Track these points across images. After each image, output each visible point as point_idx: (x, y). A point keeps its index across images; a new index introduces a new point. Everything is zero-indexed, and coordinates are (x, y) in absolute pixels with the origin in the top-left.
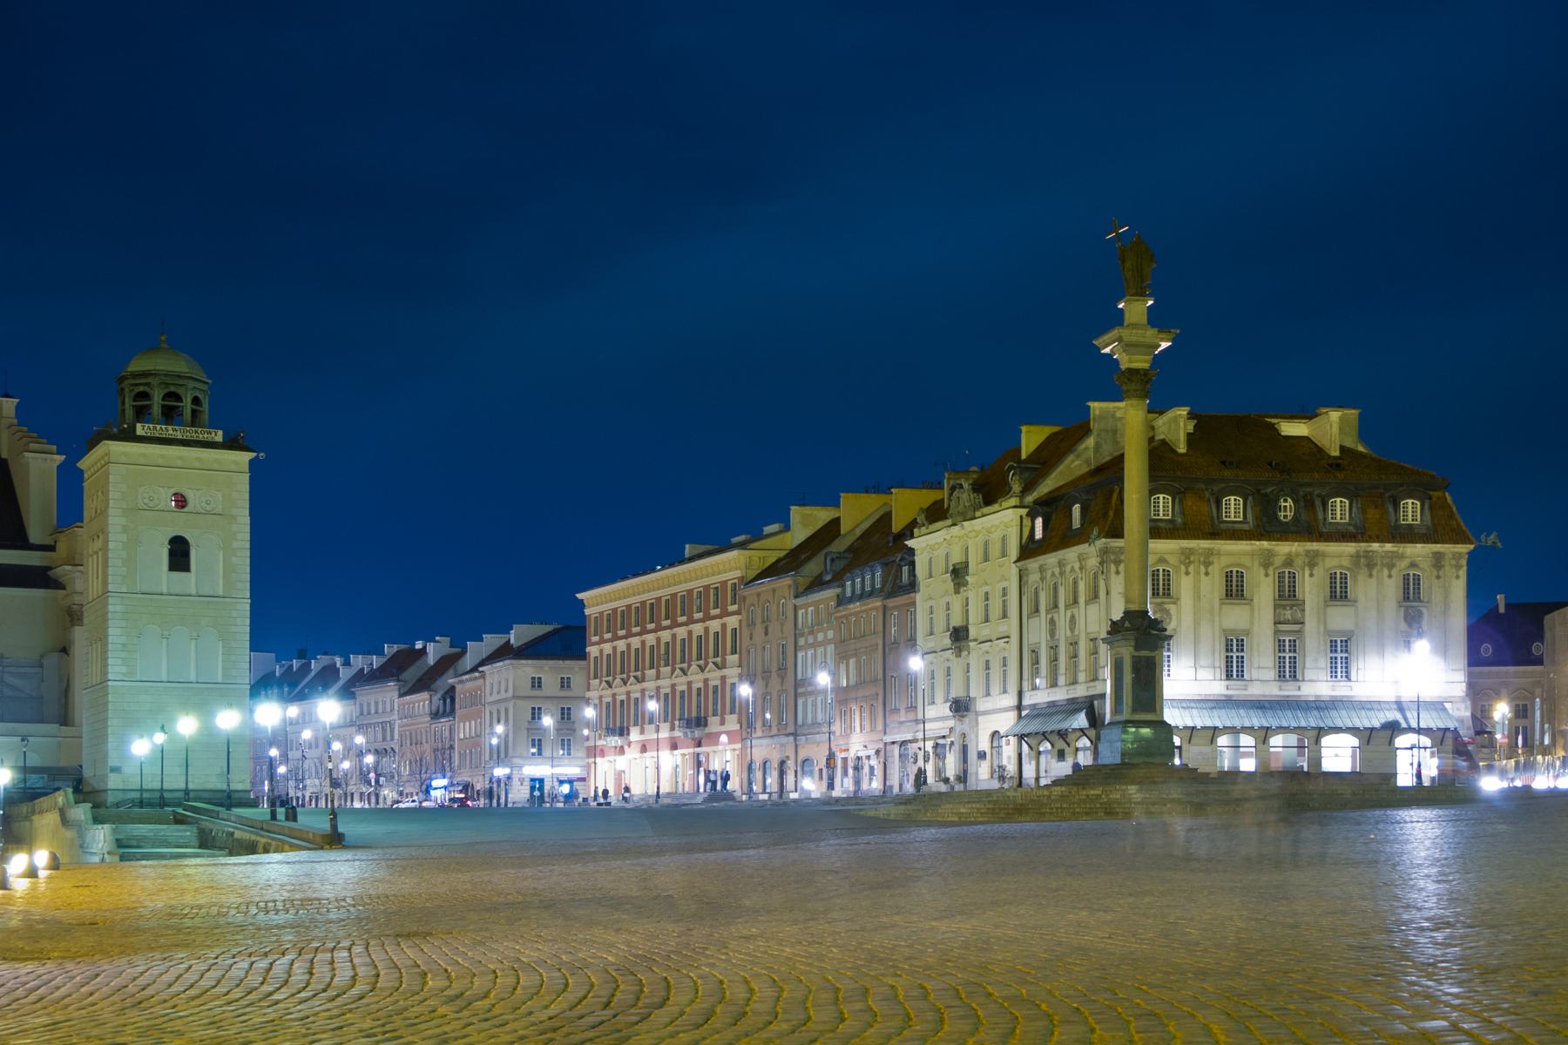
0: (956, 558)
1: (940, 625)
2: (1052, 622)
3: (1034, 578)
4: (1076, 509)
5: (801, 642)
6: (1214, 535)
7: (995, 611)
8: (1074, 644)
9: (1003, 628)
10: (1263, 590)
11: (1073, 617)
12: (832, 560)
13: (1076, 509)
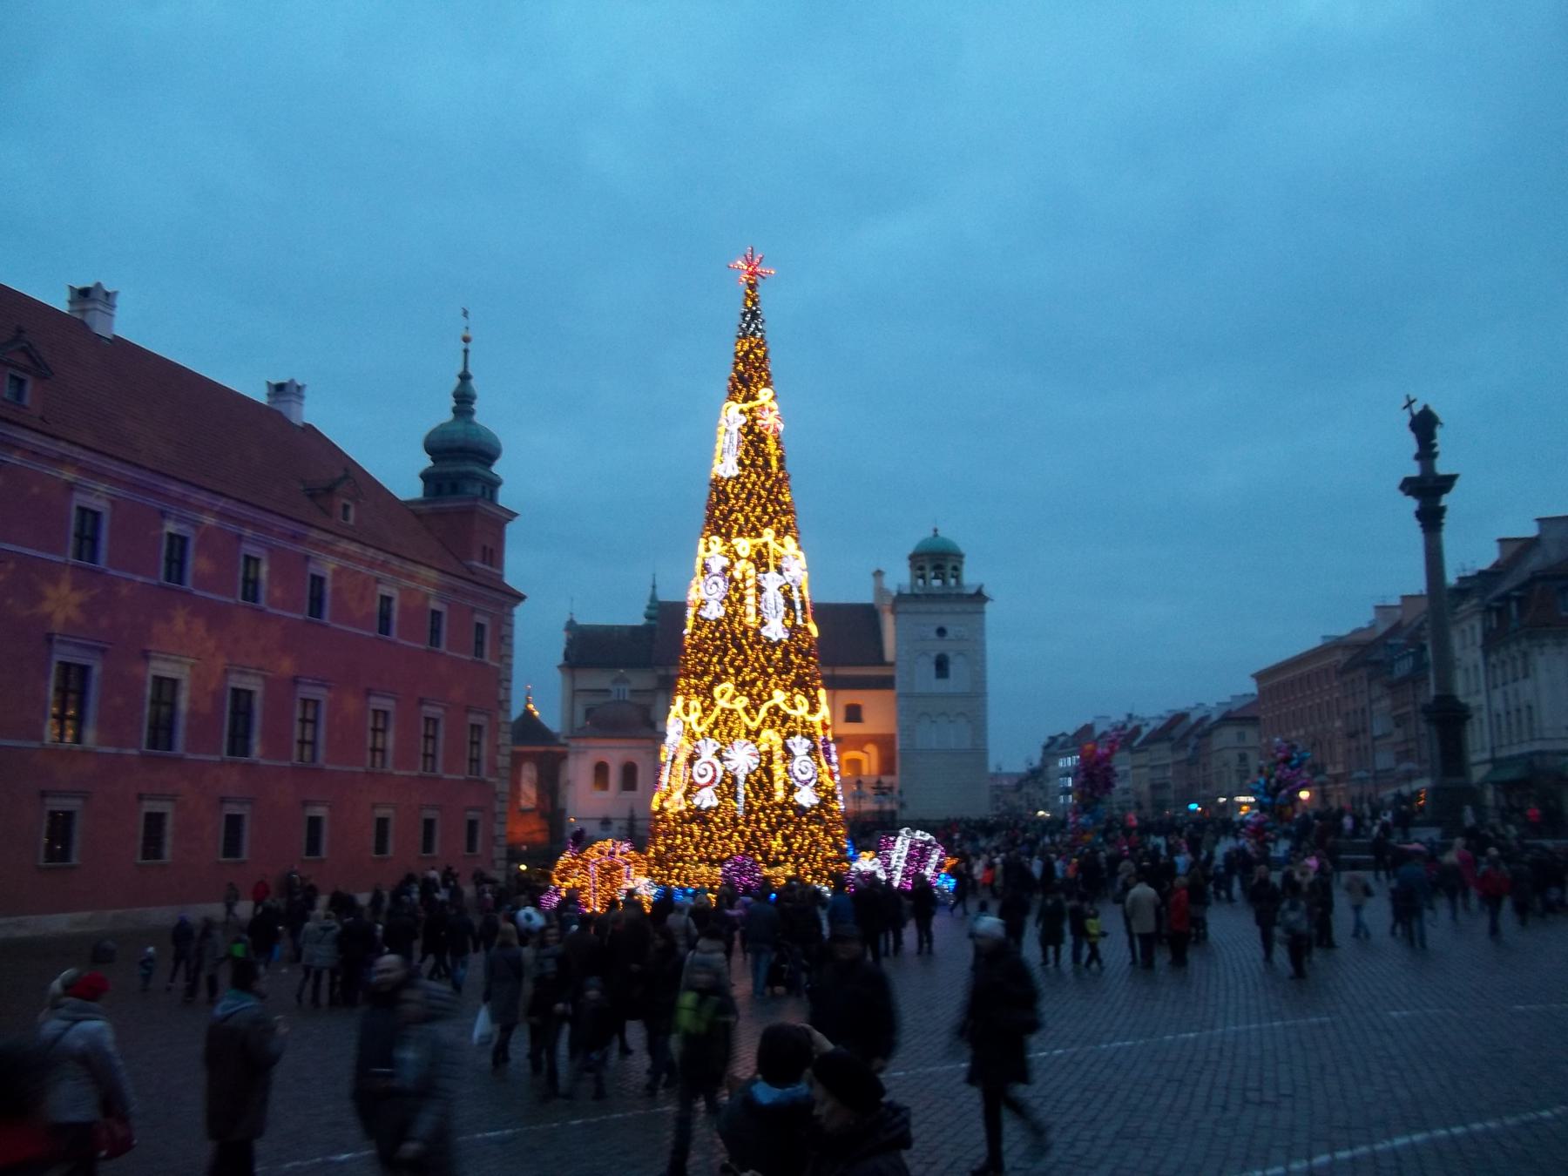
2: (1505, 693)
3: (1493, 659)
8: (1518, 710)
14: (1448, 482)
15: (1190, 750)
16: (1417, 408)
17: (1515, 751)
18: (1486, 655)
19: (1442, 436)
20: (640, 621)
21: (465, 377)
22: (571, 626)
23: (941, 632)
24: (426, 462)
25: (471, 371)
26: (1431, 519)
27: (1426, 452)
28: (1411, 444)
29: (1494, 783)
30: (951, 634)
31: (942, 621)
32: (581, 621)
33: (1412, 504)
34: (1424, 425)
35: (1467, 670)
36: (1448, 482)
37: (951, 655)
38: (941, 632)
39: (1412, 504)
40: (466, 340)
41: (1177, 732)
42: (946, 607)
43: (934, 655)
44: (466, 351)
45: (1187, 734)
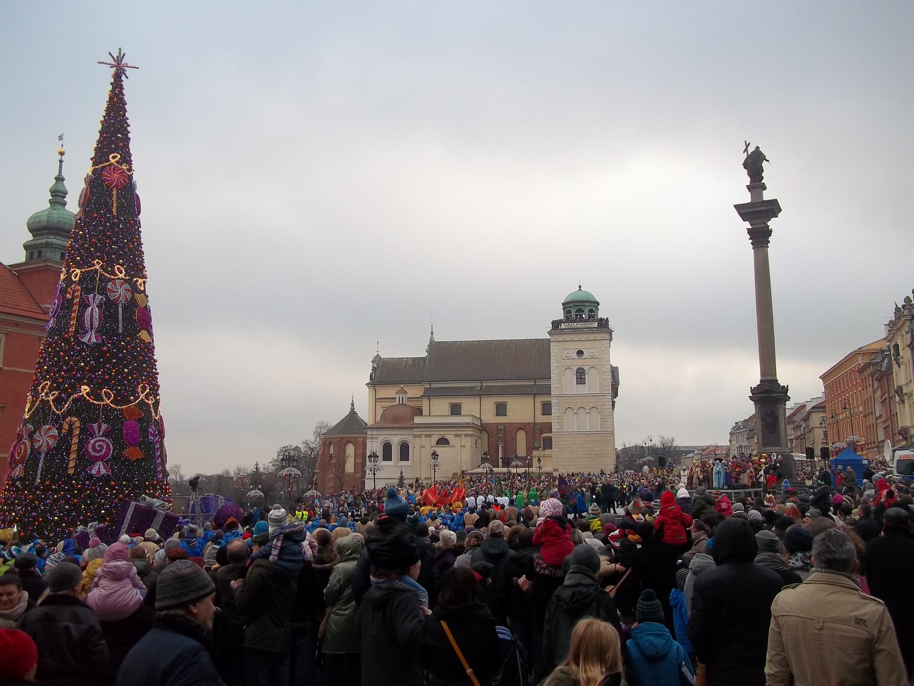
14: (773, 208)
16: (751, 149)
20: (425, 354)
21: (60, 179)
22: (377, 360)
23: (580, 353)
24: (29, 237)
25: (64, 174)
26: (760, 238)
27: (756, 183)
30: (586, 355)
31: (580, 346)
32: (384, 355)
34: (754, 164)
36: (773, 208)
37: (586, 368)
38: (580, 353)
40: (62, 154)
42: (584, 337)
43: (575, 369)
44: (61, 161)
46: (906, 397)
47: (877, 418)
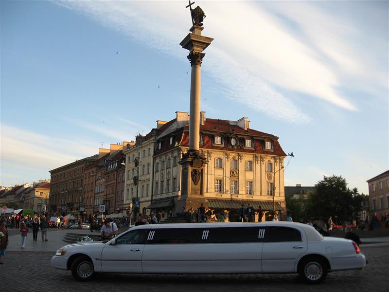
0: (136, 156)
1: (131, 177)
2: (162, 173)
3: (158, 161)
4: (171, 139)
5: (97, 182)
6: (213, 147)
7: (146, 172)
9: (148, 176)
10: (228, 165)
11: (169, 172)
12: (106, 160)
13: (171, 139)
15: (21, 198)
17: (164, 196)
18: (154, 159)
19: (205, 22)
26: (195, 59)
28: (190, 23)
29: (152, 209)
33: (187, 52)
34: (198, 16)
35: (144, 166)
39: (187, 52)
41: (18, 192)
45: (21, 193)
46: (139, 182)
47: (95, 194)
